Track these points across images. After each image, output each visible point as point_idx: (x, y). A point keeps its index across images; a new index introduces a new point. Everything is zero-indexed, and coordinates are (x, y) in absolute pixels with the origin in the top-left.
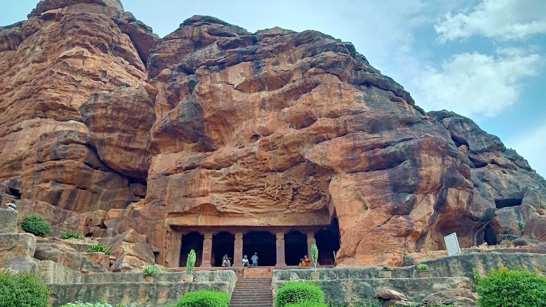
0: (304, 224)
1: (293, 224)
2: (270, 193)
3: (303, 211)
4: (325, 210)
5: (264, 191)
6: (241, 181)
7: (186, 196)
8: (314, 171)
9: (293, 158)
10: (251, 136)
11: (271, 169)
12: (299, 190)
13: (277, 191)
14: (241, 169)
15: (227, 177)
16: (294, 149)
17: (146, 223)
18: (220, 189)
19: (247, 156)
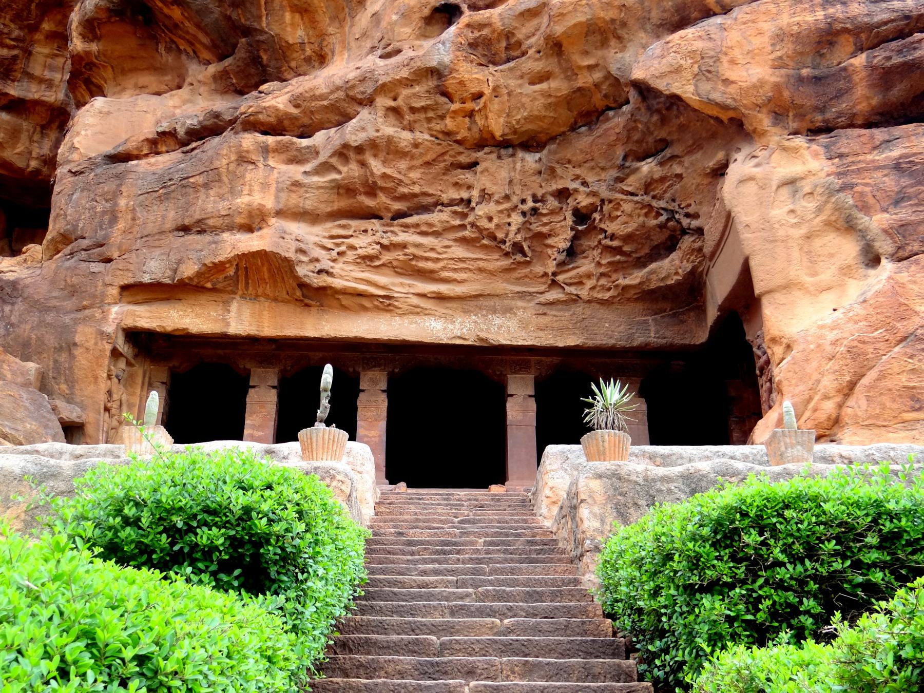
0: (611, 342)
1: (571, 341)
2: (491, 226)
3: (607, 295)
4: (692, 289)
5: (470, 219)
6: (385, 176)
7: (185, 229)
8: (662, 134)
9: (580, 89)
10: (426, 12)
11: (498, 134)
12: (597, 216)
13: (516, 219)
14: (389, 130)
15: (334, 161)
16: (586, 53)
17: (42, 324)
18: (309, 205)
19: (408, 83)
